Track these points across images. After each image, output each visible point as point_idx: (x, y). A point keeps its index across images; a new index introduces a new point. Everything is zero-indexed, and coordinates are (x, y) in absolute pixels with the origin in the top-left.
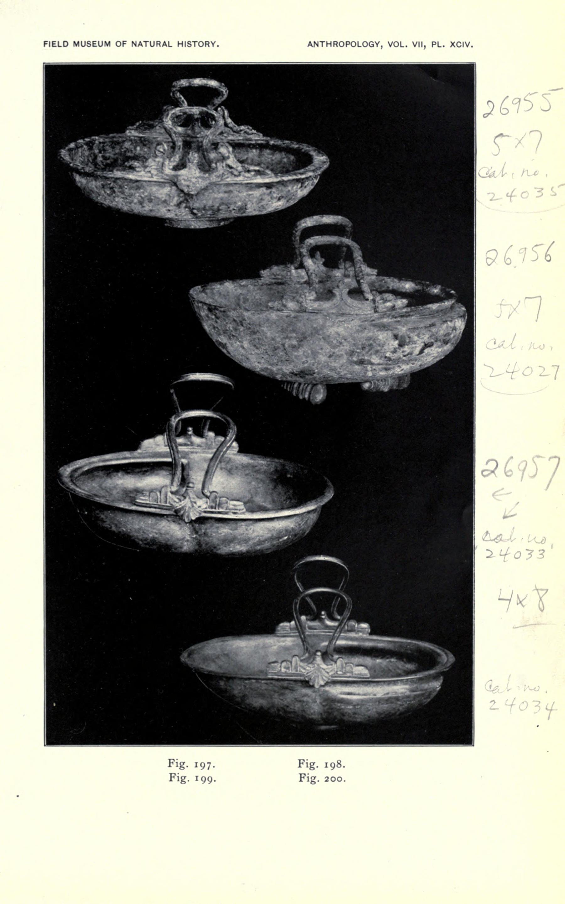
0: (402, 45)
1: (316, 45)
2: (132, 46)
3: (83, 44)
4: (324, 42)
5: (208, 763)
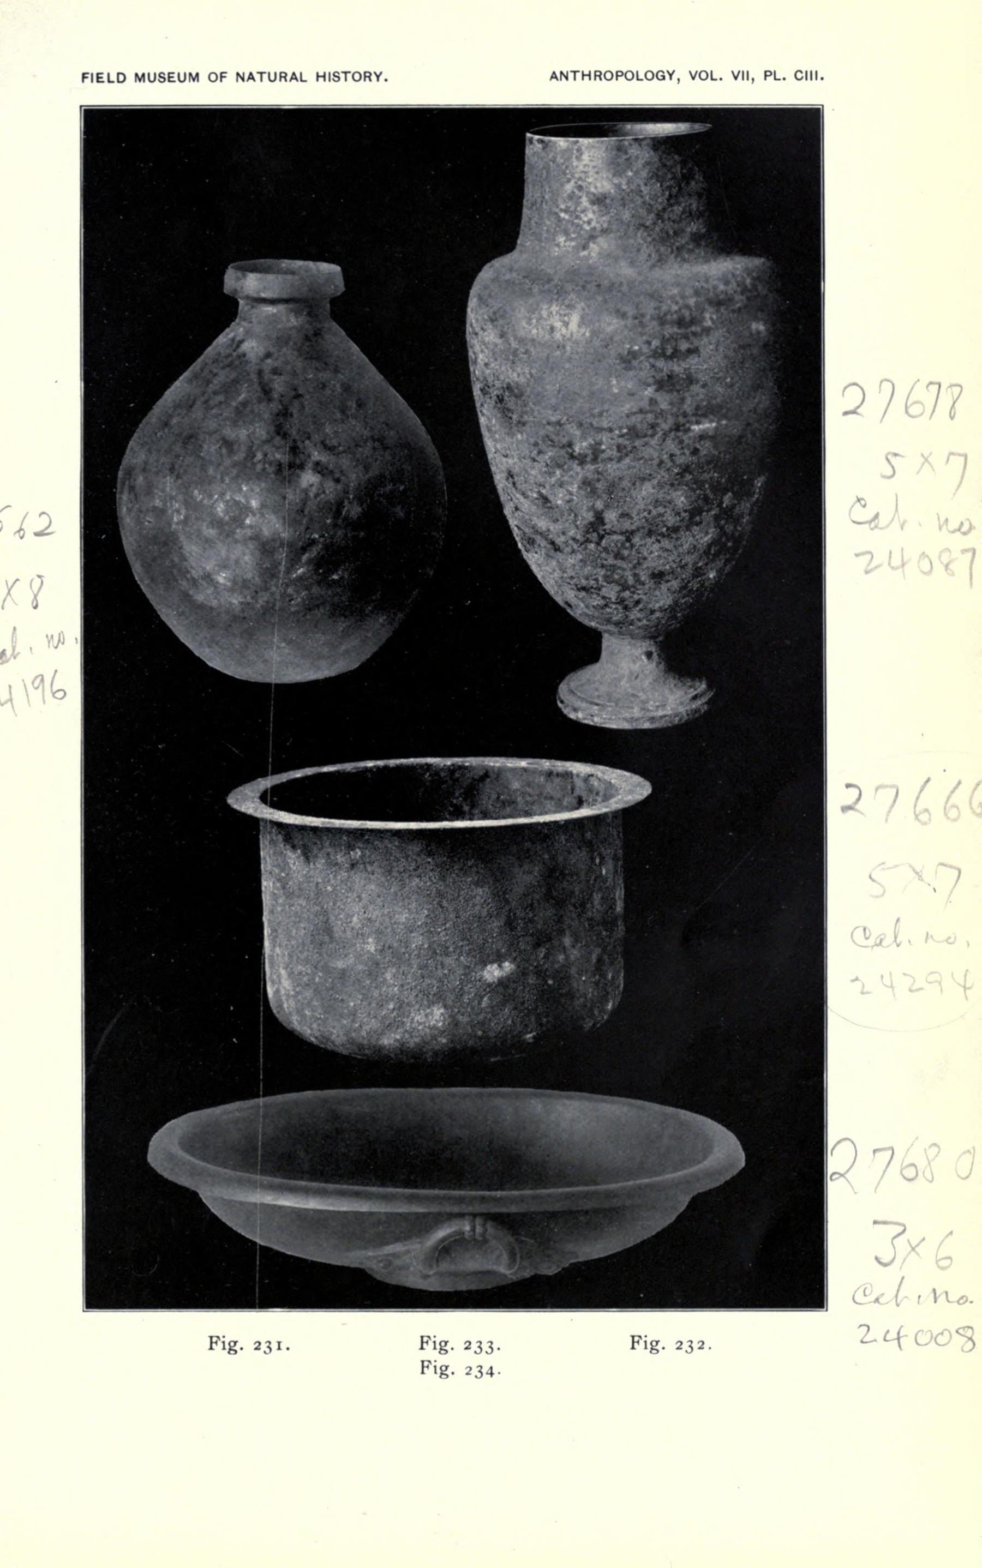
0: (714, 77)
1: (563, 77)
2: (237, 81)
3: (152, 78)
4: (578, 71)
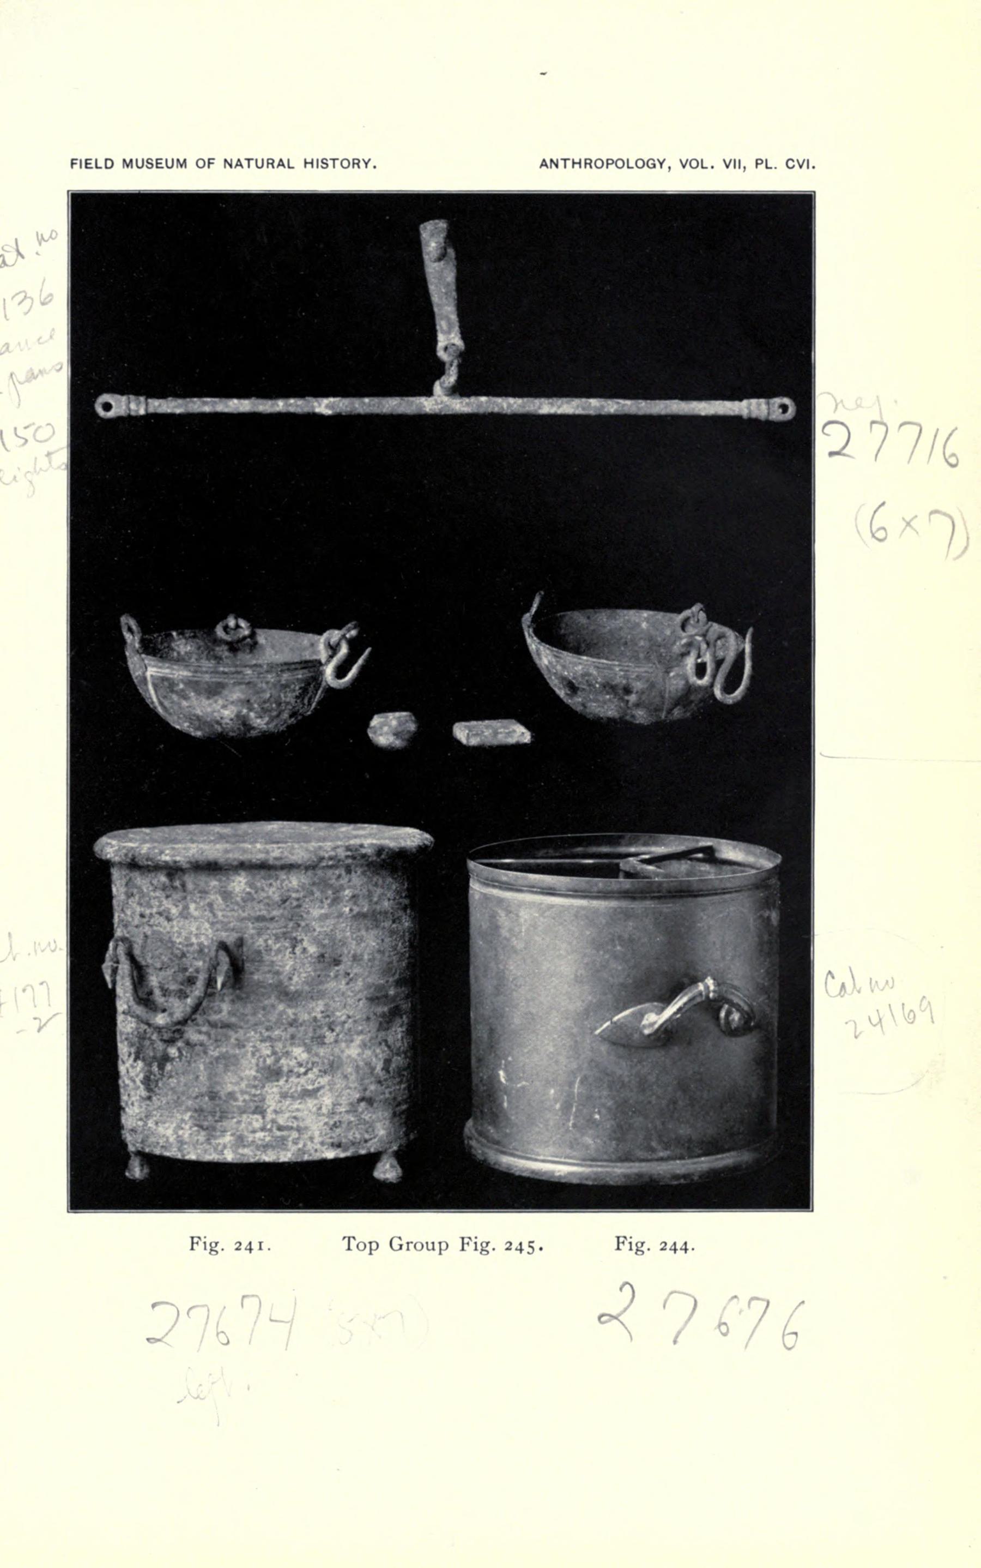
0: (704, 166)
1: (553, 165)
2: (225, 167)
3: (140, 164)
4: (569, 159)
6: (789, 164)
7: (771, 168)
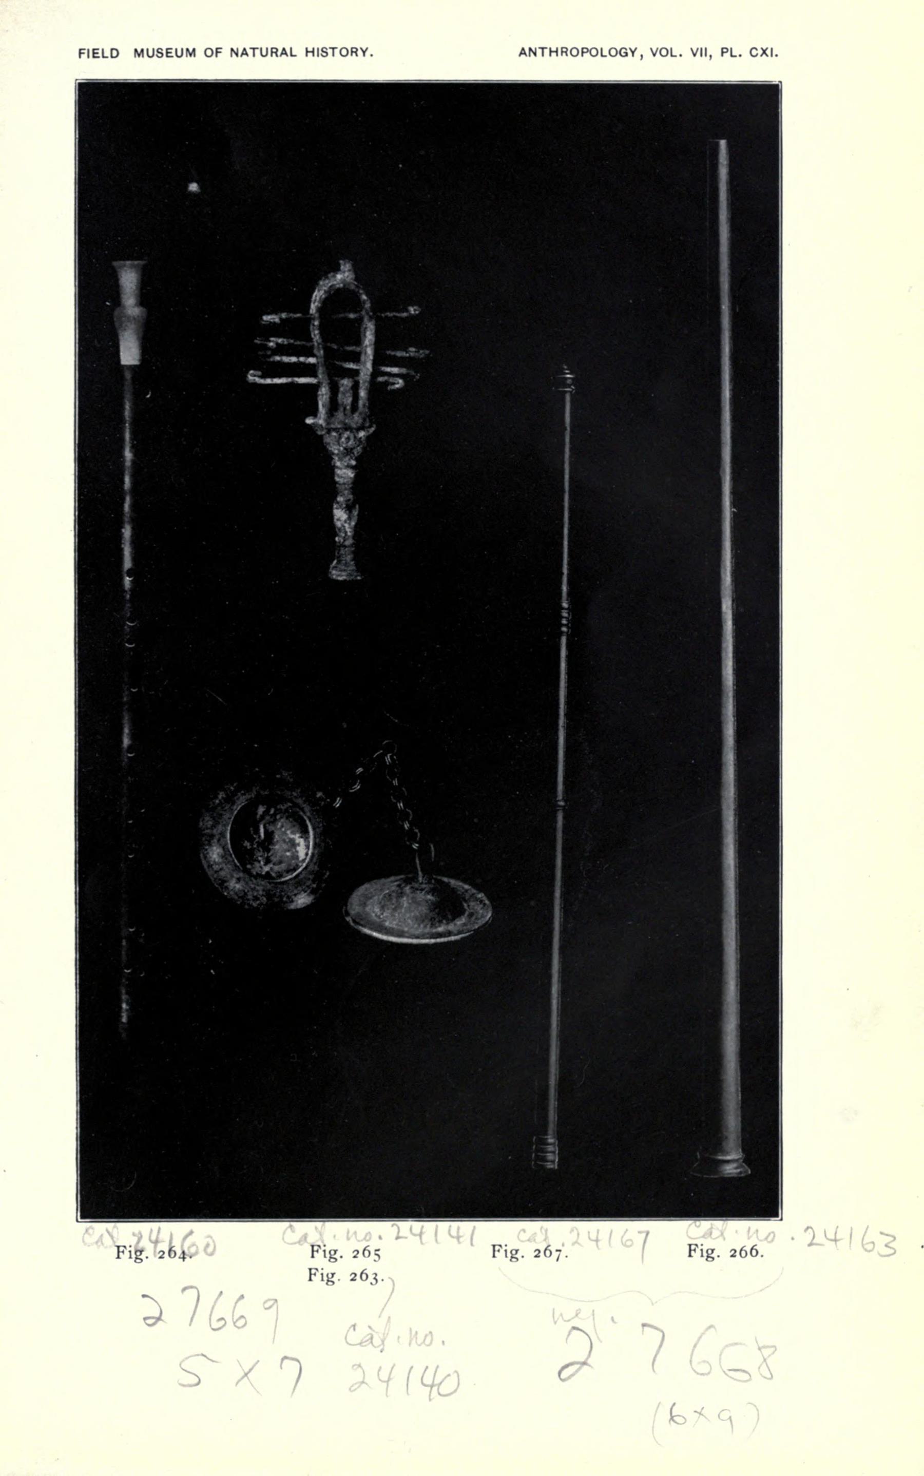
0: (674, 54)
1: (532, 54)
2: (231, 56)
3: (151, 54)
4: (546, 48)
5: (557, 1251)
6: (752, 52)
7: (735, 56)
